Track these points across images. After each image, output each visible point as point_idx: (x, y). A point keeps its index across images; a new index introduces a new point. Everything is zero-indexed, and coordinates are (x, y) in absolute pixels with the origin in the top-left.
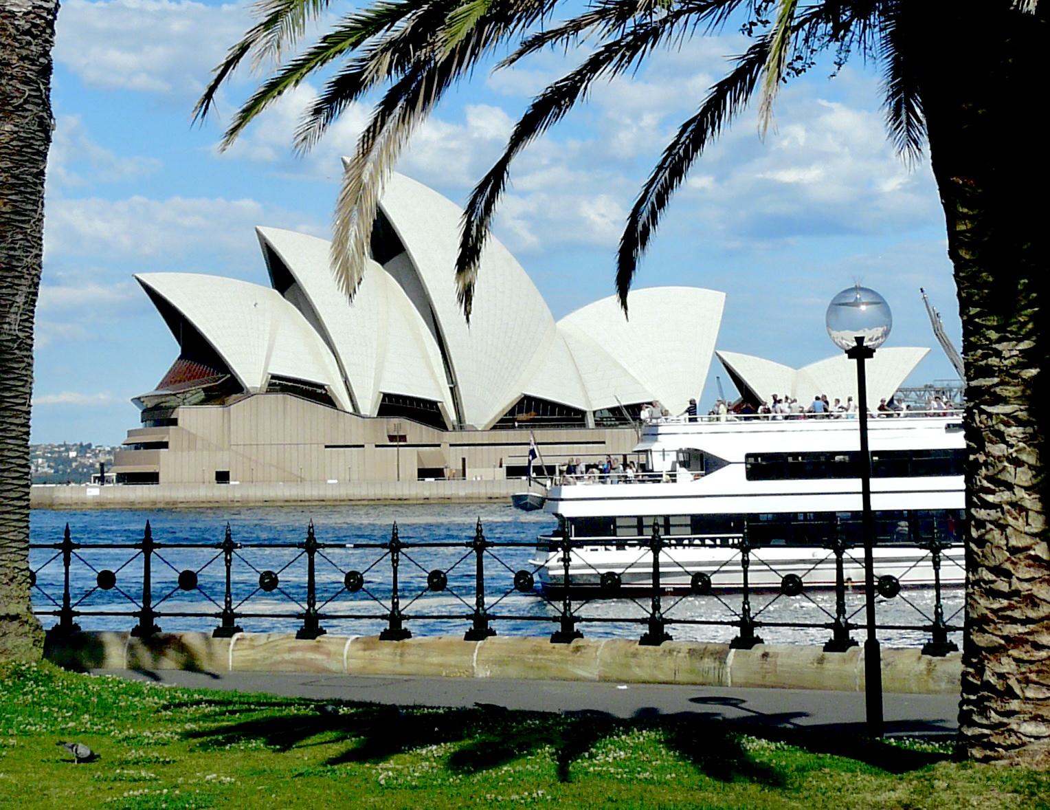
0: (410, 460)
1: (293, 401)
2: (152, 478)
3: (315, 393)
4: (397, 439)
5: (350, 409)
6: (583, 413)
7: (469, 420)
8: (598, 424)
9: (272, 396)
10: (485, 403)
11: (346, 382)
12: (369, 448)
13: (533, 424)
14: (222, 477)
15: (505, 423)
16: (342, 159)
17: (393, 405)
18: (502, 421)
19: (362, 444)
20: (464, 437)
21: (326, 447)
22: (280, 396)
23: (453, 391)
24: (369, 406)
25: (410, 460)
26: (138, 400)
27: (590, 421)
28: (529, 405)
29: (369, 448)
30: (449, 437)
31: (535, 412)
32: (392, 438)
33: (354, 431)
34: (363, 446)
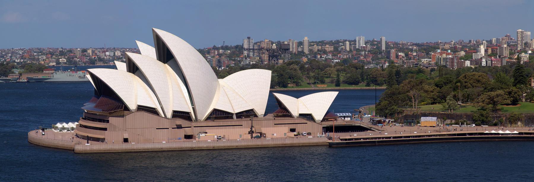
0: (182, 133)
2: (103, 140)
3: (152, 111)
4: (179, 127)
5: (164, 116)
6: (232, 114)
7: (199, 117)
8: (237, 117)
10: (204, 113)
11: (162, 108)
13: (216, 118)
14: (126, 140)
15: (208, 118)
16: (153, 30)
17: (177, 114)
23: (194, 109)
24: (169, 115)
25: (182, 133)
27: (235, 117)
28: (216, 112)
30: (194, 124)
31: (218, 115)
32: (177, 125)
33: (166, 124)
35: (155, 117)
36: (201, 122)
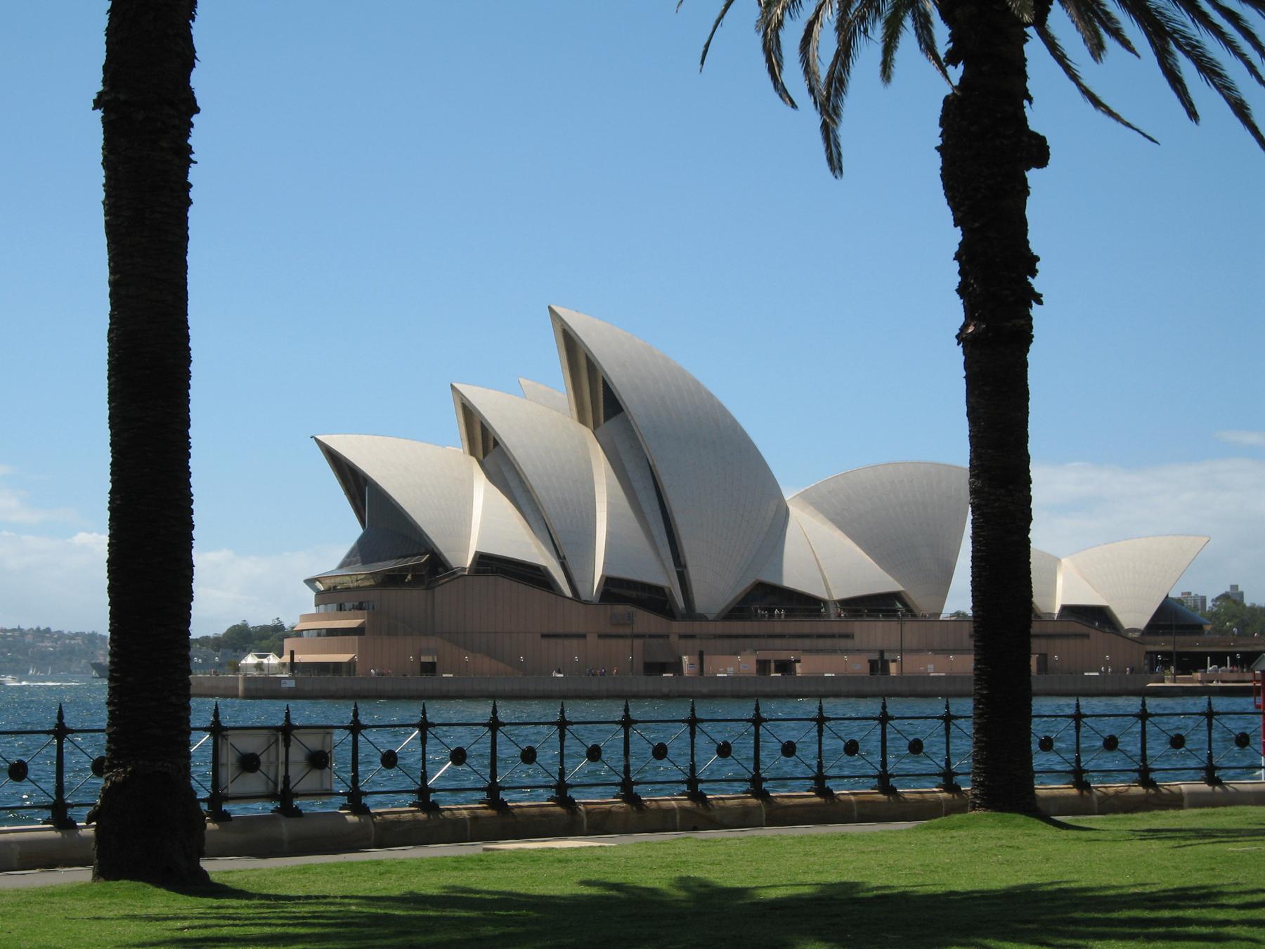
1: (507, 586)
6: (825, 602)
7: (701, 604)
9: (483, 579)
12: (592, 639)
14: (429, 669)
18: (733, 610)
19: (582, 631)
20: (696, 627)
21: (544, 636)
22: (491, 579)
26: (310, 582)
27: (833, 610)
29: (592, 639)
30: (678, 627)
34: (584, 636)
35: (538, 594)
36: (702, 618)
